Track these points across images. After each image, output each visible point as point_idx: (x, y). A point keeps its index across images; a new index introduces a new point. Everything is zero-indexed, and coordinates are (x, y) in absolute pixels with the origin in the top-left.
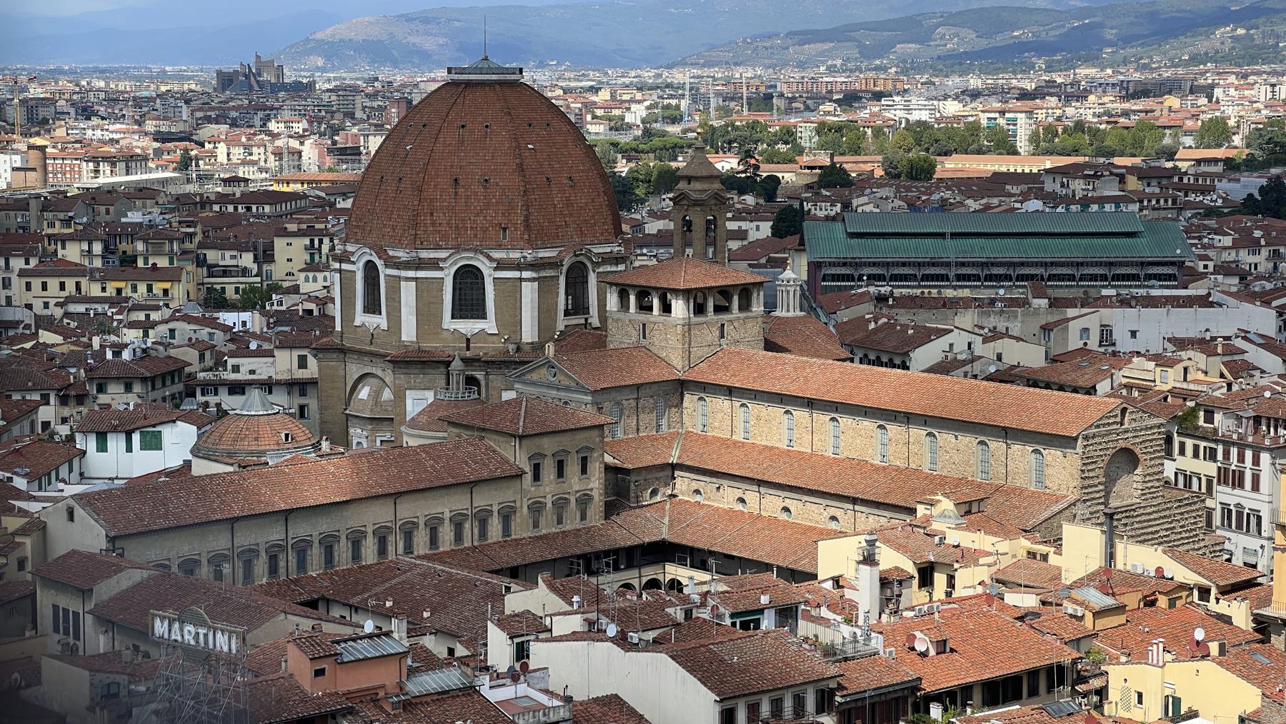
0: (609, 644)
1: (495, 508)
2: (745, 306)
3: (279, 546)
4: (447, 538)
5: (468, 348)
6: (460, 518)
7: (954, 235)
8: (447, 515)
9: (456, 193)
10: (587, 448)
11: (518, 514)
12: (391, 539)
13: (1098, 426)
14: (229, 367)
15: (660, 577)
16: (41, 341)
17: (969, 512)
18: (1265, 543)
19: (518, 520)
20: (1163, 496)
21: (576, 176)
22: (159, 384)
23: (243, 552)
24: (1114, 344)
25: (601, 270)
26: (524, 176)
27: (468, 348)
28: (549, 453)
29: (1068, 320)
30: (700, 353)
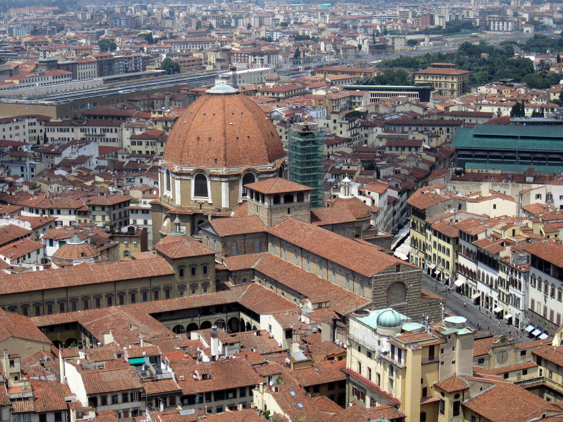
0: (74, 368)
1: (162, 287)
2: (301, 199)
3: (64, 300)
4: (139, 299)
5: (201, 209)
6: (145, 291)
7: (522, 138)
8: (139, 289)
9: (198, 144)
10: (206, 263)
11: (173, 290)
12: (113, 298)
13: (383, 273)
14: (142, 202)
15: (237, 317)
16: (96, 180)
17: (320, 307)
18: (521, 312)
19: (173, 292)
20: (421, 301)
21: (251, 136)
22: (122, 206)
23: (47, 302)
24: (553, 201)
25: (261, 176)
26: (225, 137)
27: (201, 209)
28: (187, 265)
29: (532, 189)
30: (276, 220)
